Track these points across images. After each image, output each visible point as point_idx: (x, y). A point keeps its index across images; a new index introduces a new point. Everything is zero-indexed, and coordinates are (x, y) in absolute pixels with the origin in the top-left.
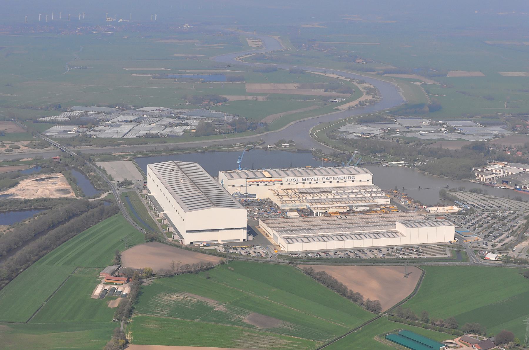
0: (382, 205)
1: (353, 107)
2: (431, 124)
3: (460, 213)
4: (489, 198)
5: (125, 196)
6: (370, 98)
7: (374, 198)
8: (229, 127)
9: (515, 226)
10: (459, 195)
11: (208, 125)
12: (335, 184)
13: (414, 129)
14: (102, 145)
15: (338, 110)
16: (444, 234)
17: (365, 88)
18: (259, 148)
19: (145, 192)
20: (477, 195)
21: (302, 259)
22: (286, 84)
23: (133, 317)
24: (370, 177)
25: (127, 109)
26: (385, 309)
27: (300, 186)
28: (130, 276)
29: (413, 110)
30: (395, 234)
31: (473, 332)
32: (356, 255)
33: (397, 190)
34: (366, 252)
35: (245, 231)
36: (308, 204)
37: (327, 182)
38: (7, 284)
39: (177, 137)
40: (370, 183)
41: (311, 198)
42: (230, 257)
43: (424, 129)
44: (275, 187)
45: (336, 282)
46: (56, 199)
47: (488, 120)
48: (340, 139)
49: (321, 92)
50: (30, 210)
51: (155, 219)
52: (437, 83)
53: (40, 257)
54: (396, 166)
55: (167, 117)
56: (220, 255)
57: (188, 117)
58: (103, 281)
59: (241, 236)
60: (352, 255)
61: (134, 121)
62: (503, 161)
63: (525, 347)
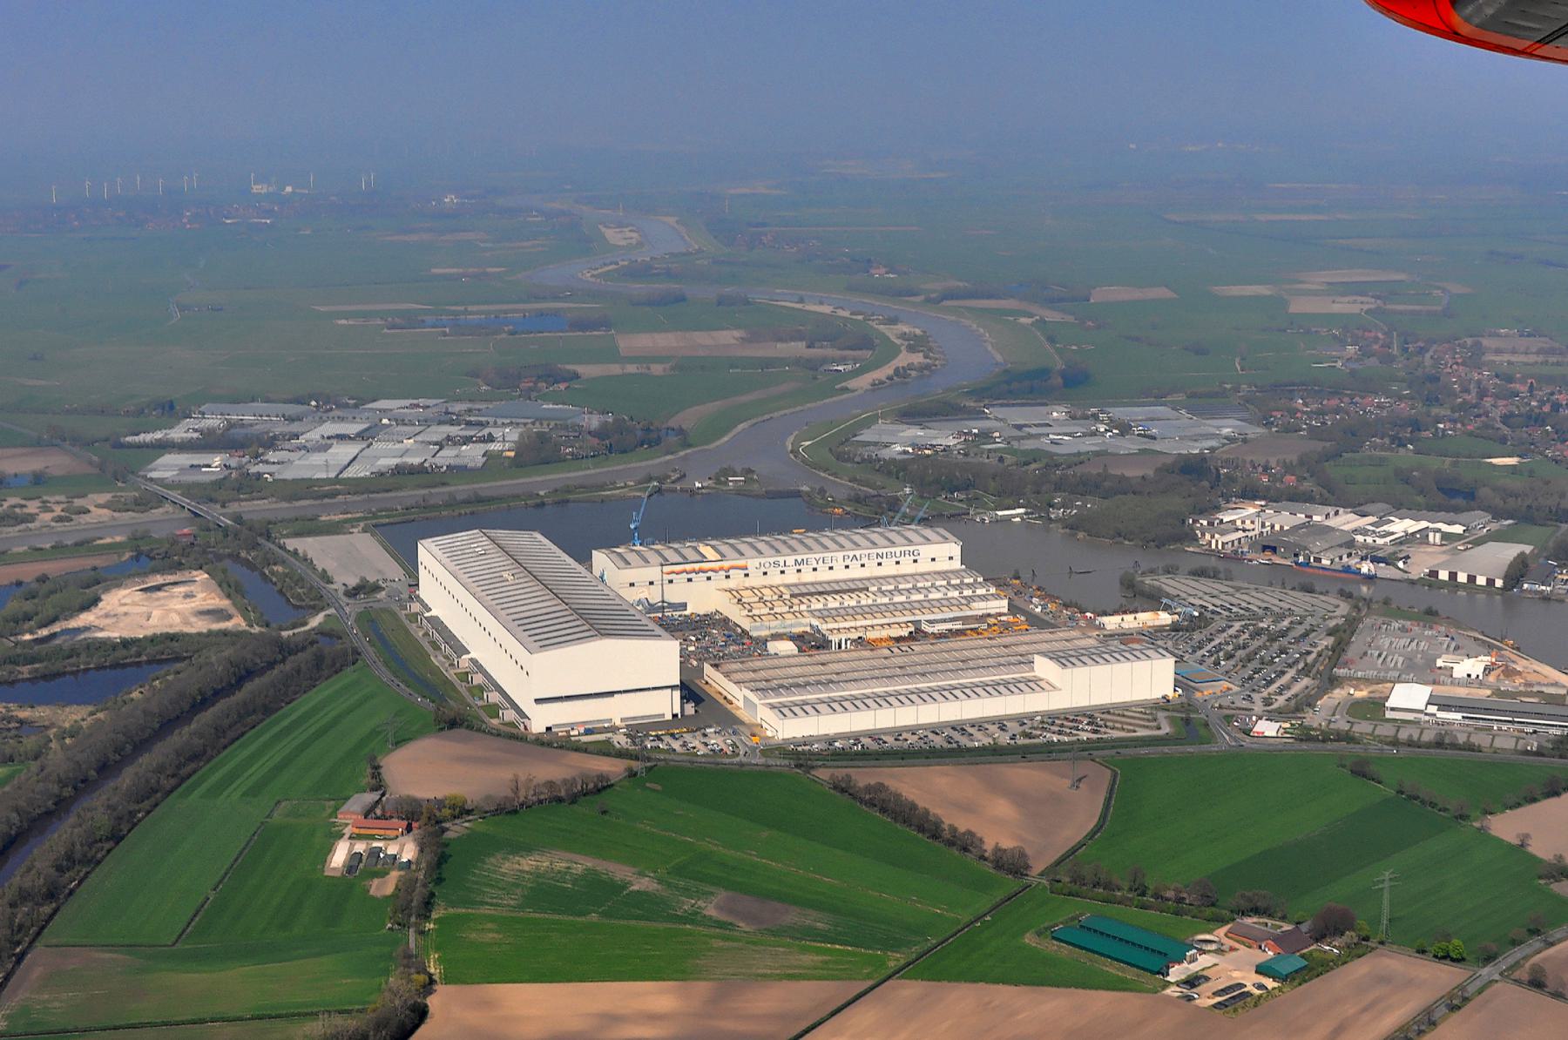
0: (989, 615)
1: (882, 382)
2: (1073, 418)
3: (1175, 628)
4: (1238, 589)
5: (369, 620)
6: (918, 359)
7: (969, 599)
8: (595, 441)
9: (1309, 653)
10: (1168, 584)
11: (541, 436)
12: (872, 570)
13: (1034, 431)
14: (292, 498)
15: (846, 390)
16: (1149, 679)
17: (903, 336)
18: (675, 491)
19: (416, 607)
20: (1209, 582)
21: (818, 755)
22: (715, 334)
23: (434, 915)
24: (955, 549)
25: (339, 406)
26: (1038, 866)
27: (791, 577)
28: (412, 815)
29: (1027, 386)
30: (1034, 684)
31: (1256, 911)
32: (949, 740)
33: (1017, 578)
34: (971, 730)
35: (677, 694)
36: (815, 622)
37: (855, 565)
38: (109, 851)
39: (472, 470)
40: (956, 564)
41: (820, 606)
42: (649, 759)
43: (1057, 430)
44: (731, 584)
45: (913, 807)
46: (199, 634)
47: (1205, 402)
48: (863, 460)
49: (798, 348)
50: (139, 664)
51: (451, 674)
52: (1071, 319)
53: (183, 780)
54: (1008, 519)
55: (440, 423)
56: (621, 754)
57: (491, 420)
58: (348, 831)
59: (667, 705)
60: (938, 741)
61: (361, 436)
62: (1254, 498)
63: (1382, 943)
